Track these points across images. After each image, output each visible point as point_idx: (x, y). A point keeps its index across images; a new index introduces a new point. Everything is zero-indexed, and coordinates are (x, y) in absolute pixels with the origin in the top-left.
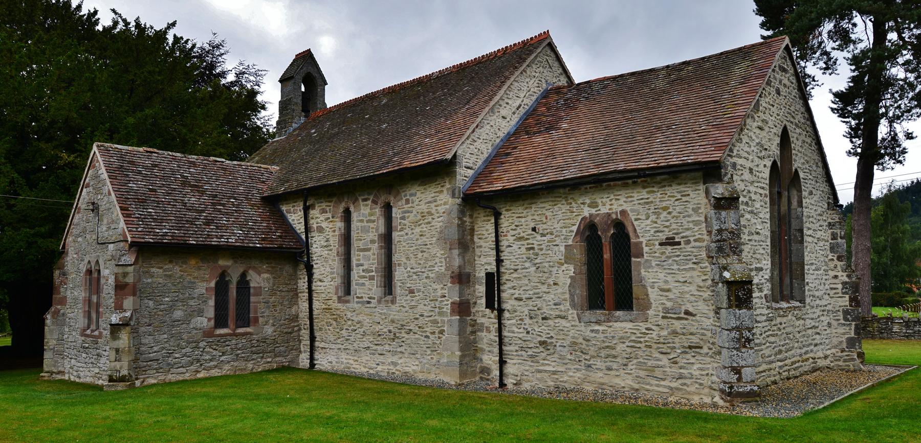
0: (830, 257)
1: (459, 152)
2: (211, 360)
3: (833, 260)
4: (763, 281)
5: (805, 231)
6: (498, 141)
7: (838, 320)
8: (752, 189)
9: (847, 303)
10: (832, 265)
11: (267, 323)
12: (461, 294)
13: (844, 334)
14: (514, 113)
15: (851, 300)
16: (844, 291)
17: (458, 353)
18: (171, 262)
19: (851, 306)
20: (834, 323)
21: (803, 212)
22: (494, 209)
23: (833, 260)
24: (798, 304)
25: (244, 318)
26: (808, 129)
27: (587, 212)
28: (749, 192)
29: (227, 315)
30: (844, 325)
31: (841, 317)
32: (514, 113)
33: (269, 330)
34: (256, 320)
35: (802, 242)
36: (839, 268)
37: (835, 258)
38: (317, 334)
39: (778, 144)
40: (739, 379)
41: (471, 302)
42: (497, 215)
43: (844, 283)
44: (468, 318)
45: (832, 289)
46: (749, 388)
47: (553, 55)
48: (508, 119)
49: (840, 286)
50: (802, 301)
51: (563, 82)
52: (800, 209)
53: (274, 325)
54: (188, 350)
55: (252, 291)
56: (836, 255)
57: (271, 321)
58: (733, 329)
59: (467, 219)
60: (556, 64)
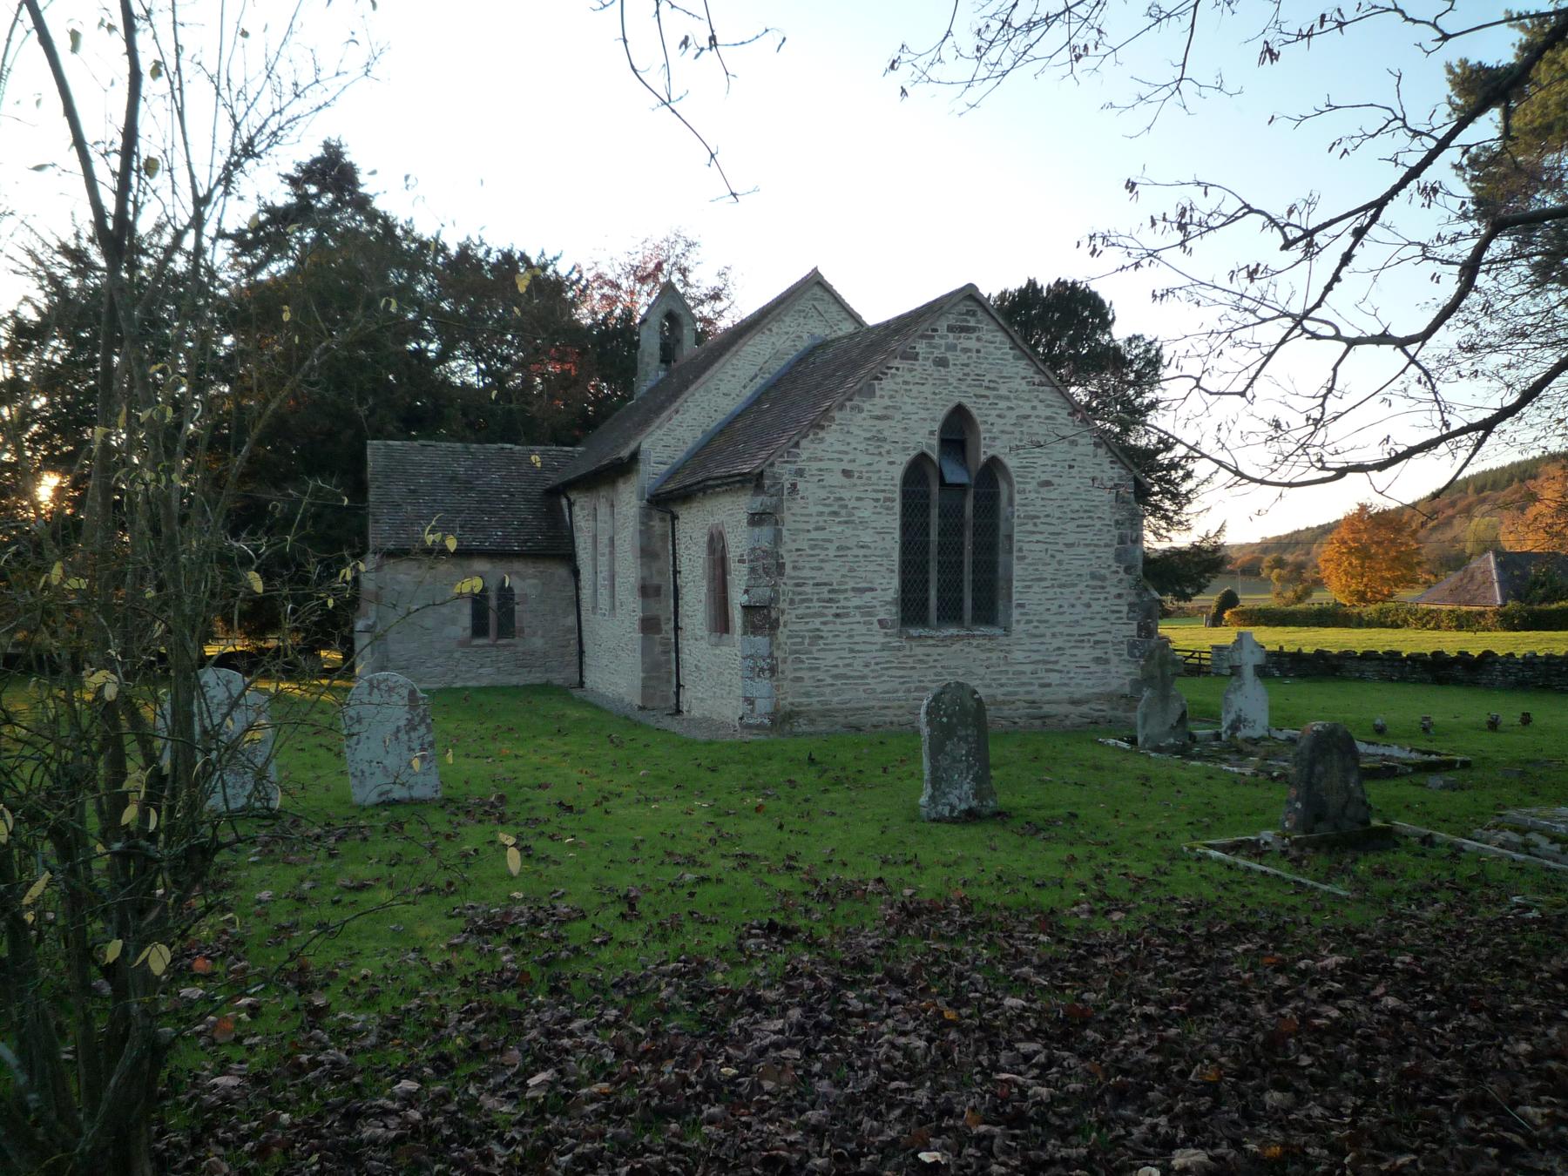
0: (1114, 569)
1: (644, 446)
2: (467, 672)
3: (1117, 572)
4: (875, 603)
5: (1016, 537)
6: (714, 424)
7: (1120, 655)
8: (846, 494)
9: (1135, 633)
10: (1115, 578)
11: (534, 634)
12: (643, 611)
13: (1128, 674)
14: (745, 387)
15: (1140, 628)
16: (1131, 615)
17: (641, 675)
18: (419, 568)
19: (1139, 636)
20: (1115, 660)
21: (1013, 513)
22: (672, 512)
23: (1117, 572)
24: (1001, 631)
25: (507, 627)
26: (1042, 396)
27: (711, 521)
28: (841, 499)
29: (487, 624)
30: (1128, 661)
31: (1126, 652)
32: (745, 387)
33: (538, 642)
34: (522, 630)
35: (1010, 551)
36: (1125, 584)
37: (1121, 571)
38: (586, 648)
39: (932, 433)
40: (752, 711)
41: (662, 618)
42: (674, 518)
43: (1131, 605)
44: (657, 637)
45: (1113, 612)
46: (759, 720)
47: (826, 296)
48: (733, 395)
49: (1125, 609)
50: (1007, 630)
51: (848, 328)
52: (1010, 509)
53: (543, 637)
54: (441, 660)
55: (517, 599)
56: (1123, 566)
57: (540, 632)
58: (748, 657)
59: (657, 525)
60: (834, 308)
